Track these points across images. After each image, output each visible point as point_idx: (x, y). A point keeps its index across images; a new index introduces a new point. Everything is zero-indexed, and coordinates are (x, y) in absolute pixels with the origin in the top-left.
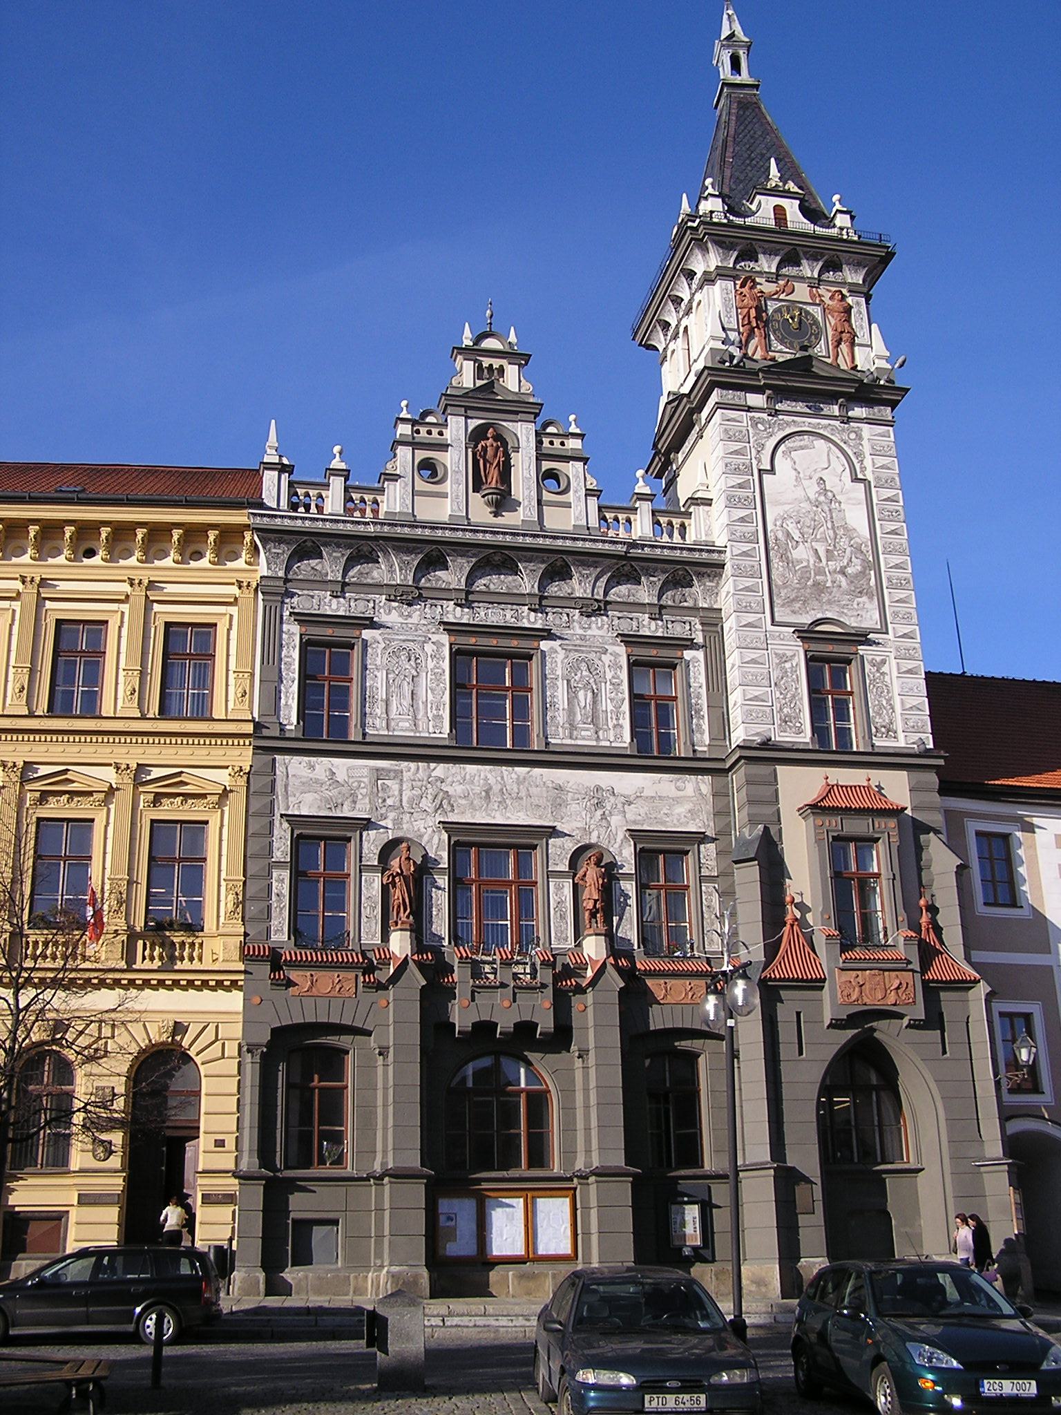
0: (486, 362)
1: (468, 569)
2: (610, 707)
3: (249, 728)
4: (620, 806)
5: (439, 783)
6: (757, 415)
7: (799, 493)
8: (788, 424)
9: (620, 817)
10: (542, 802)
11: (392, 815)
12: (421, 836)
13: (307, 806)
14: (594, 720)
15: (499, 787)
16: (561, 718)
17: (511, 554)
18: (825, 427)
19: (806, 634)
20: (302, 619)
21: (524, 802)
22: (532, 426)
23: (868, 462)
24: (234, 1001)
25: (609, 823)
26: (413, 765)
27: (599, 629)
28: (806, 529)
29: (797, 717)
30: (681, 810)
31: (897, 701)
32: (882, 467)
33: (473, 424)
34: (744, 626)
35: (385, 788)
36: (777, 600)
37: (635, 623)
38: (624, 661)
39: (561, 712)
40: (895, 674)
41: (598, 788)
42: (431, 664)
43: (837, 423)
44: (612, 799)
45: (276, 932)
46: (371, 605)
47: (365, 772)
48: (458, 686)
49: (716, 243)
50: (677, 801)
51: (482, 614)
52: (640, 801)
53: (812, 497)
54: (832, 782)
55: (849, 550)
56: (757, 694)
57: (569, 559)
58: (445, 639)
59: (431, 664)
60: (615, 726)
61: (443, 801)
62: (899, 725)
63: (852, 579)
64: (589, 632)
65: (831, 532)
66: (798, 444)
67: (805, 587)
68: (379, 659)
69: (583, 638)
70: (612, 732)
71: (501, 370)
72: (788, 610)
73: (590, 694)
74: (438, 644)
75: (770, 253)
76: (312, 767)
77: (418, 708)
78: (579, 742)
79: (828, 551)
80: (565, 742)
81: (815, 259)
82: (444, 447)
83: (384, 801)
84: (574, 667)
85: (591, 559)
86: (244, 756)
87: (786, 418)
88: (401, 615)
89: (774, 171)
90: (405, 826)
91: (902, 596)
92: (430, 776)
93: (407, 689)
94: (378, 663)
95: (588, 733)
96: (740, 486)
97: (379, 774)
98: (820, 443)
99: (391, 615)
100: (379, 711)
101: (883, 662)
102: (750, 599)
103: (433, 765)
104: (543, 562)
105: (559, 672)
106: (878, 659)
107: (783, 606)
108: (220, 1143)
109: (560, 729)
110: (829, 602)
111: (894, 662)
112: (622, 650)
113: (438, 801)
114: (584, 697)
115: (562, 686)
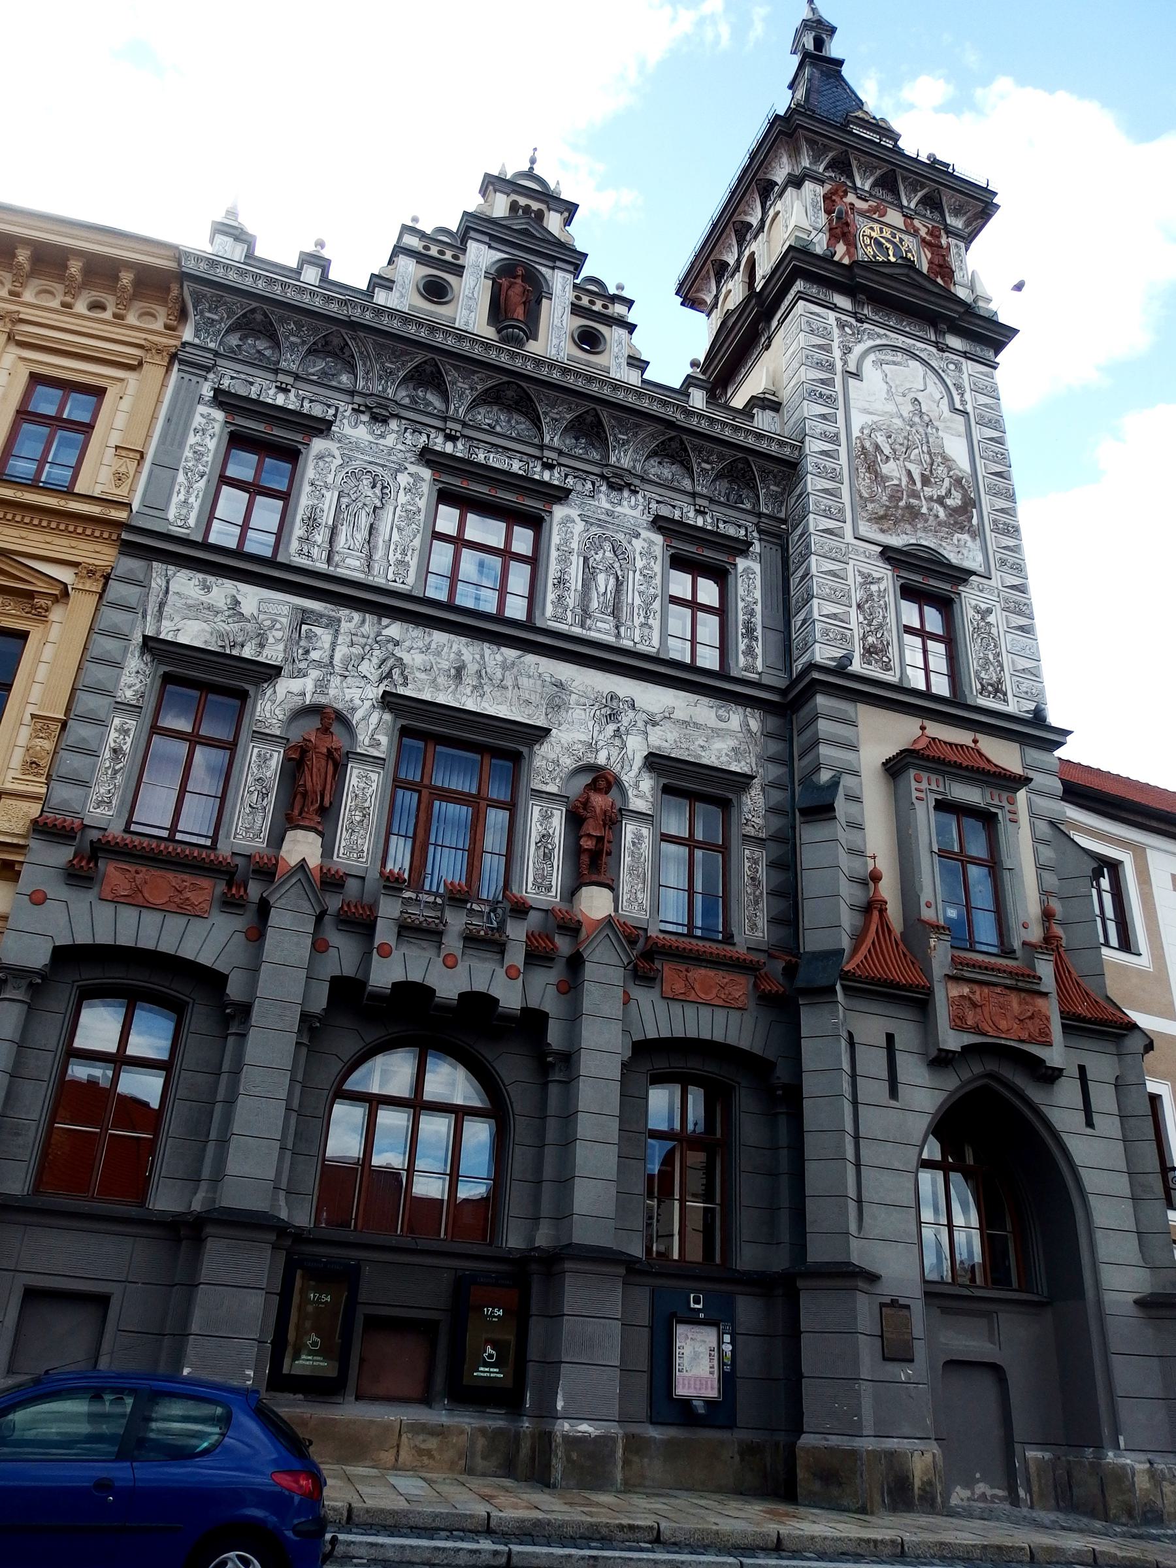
0: (523, 201)
2: (638, 601)
3: (121, 515)
4: (640, 724)
5: (390, 646)
6: (844, 318)
7: (890, 408)
8: (879, 336)
10: (533, 698)
11: (315, 674)
12: (354, 709)
14: (615, 612)
15: (476, 667)
16: (572, 600)
21: (509, 694)
22: (570, 277)
23: (967, 396)
25: (624, 746)
26: (357, 616)
27: (632, 510)
29: (884, 651)
31: (1006, 659)
41: (613, 697)
43: (934, 350)
45: (99, 804)
47: (285, 610)
49: (807, 140)
50: (717, 733)
52: (667, 725)
53: (905, 414)
55: (947, 481)
59: (403, 498)
60: (642, 625)
61: (392, 668)
62: (1008, 686)
64: (619, 509)
65: (927, 457)
66: (889, 358)
67: (897, 507)
69: (610, 513)
70: (637, 632)
72: (875, 527)
73: (612, 581)
75: (867, 170)
76: (207, 588)
77: (375, 547)
81: (914, 188)
83: (307, 652)
84: (594, 544)
87: (877, 329)
88: (372, 433)
90: (332, 692)
91: (1011, 544)
92: (379, 634)
93: (364, 521)
94: (330, 479)
95: (607, 626)
97: (304, 617)
99: (356, 431)
100: (320, 537)
101: (989, 611)
102: (831, 503)
103: (385, 621)
104: (570, 410)
105: (575, 545)
106: (984, 606)
107: (869, 520)
109: (569, 613)
110: (925, 529)
113: (385, 669)
115: (576, 563)
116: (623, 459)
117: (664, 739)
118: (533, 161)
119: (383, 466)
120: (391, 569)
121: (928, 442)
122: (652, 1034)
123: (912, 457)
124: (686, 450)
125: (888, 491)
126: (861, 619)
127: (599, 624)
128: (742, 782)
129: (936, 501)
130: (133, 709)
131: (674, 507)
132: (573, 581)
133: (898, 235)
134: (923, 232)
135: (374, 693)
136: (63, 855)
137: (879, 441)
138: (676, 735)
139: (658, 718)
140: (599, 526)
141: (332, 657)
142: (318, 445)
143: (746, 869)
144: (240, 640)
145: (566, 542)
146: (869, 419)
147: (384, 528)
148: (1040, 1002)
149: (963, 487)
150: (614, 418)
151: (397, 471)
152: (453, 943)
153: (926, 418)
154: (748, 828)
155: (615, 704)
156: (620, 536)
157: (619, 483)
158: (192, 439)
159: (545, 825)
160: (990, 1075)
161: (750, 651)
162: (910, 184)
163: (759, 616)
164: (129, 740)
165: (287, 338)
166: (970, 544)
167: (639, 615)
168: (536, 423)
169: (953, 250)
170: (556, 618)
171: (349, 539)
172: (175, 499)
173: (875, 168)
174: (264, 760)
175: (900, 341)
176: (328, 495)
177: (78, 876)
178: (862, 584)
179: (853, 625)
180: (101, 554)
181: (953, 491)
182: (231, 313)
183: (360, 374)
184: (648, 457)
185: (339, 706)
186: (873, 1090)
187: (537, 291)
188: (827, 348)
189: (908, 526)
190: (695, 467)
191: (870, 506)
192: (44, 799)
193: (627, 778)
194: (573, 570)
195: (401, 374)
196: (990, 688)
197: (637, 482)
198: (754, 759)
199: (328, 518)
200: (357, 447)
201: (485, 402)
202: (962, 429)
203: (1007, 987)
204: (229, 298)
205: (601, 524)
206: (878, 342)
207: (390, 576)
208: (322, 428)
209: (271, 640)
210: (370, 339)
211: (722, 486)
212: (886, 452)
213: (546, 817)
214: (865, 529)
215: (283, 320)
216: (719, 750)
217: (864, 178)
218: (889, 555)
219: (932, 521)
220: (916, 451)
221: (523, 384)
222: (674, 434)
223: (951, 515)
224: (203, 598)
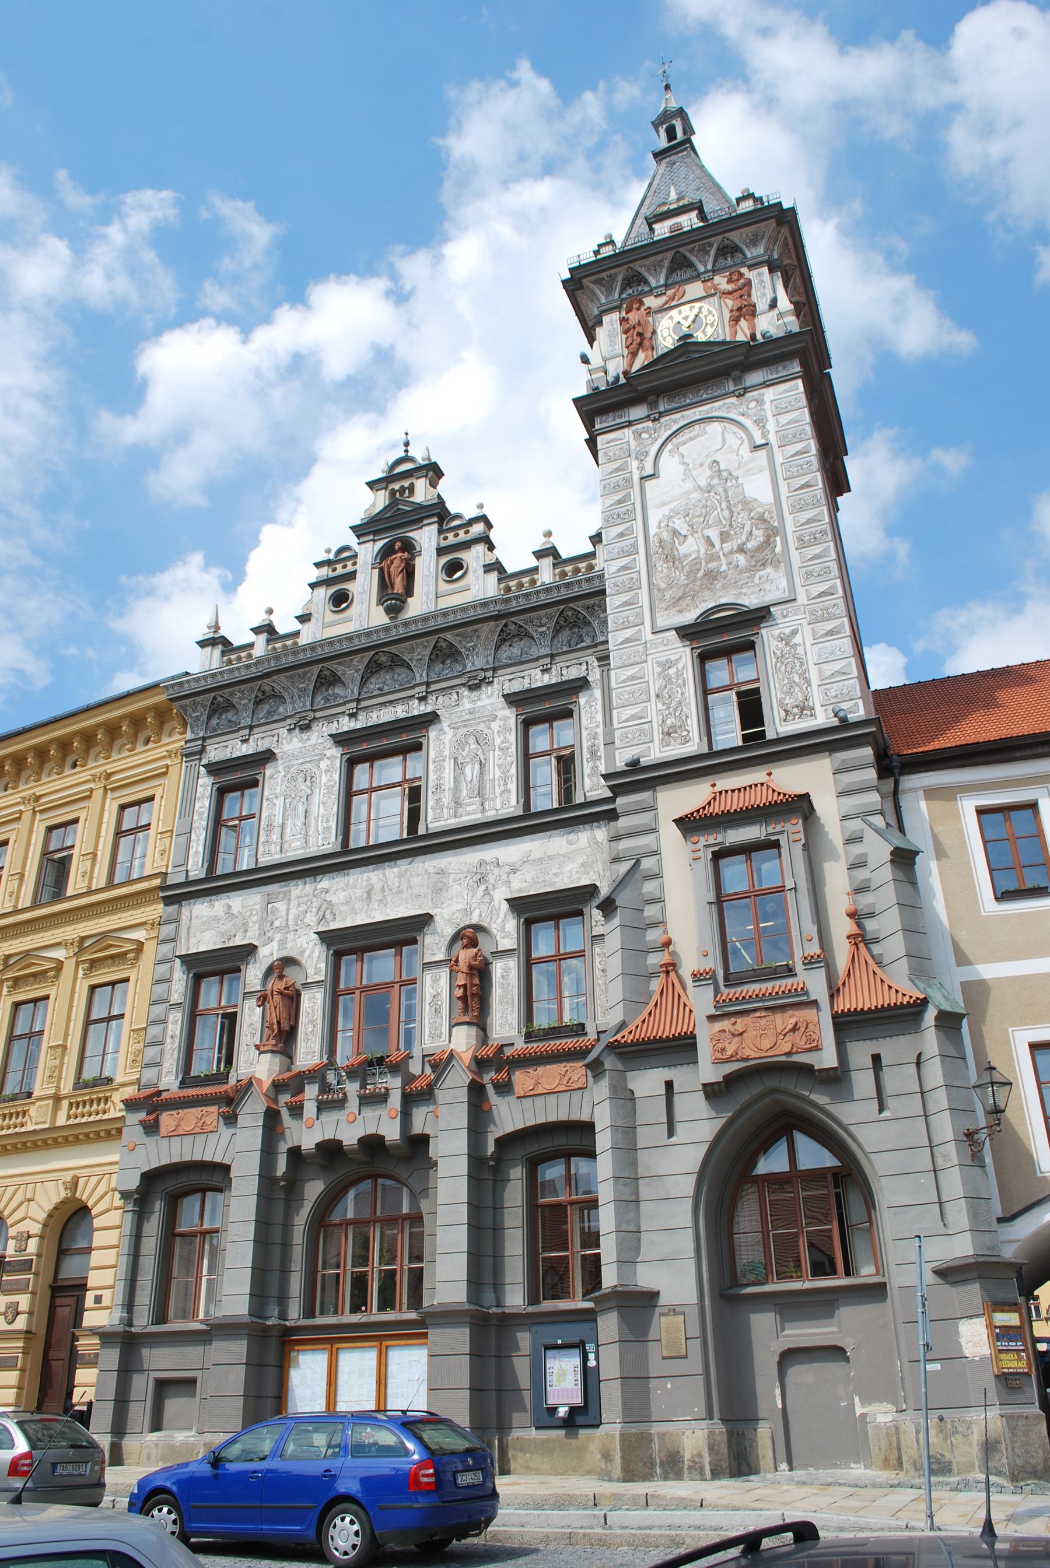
1: (359, 679)
2: (498, 774)
4: (504, 877)
5: (323, 895)
7: (690, 485)
8: (675, 422)
9: (504, 889)
11: (278, 937)
12: (303, 952)
13: (204, 941)
15: (381, 884)
16: (447, 798)
17: (392, 649)
18: (720, 408)
20: (214, 769)
21: (404, 895)
23: (771, 426)
27: (490, 698)
28: (696, 520)
32: (789, 423)
33: (380, 544)
34: (621, 643)
37: (527, 681)
39: (446, 793)
40: (809, 640)
43: (733, 400)
44: (496, 871)
46: (276, 739)
49: (594, 282)
50: (568, 856)
51: (375, 717)
53: (703, 483)
54: (717, 789)
56: (633, 712)
57: (448, 636)
59: (324, 779)
60: (502, 793)
62: (817, 700)
64: (479, 704)
65: (726, 513)
68: (278, 788)
69: (472, 712)
70: (498, 800)
72: (673, 611)
73: (477, 767)
75: (655, 269)
77: (309, 826)
78: (464, 819)
79: (722, 534)
80: (450, 822)
82: (351, 576)
83: (272, 923)
84: (461, 744)
85: (469, 629)
88: (301, 740)
90: (289, 945)
94: (278, 791)
95: (474, 807)
96: (620, 502)
98: (715, 427)
99: (290, 745)
100: (275, 837)
101: (794, 633)
105: (447, 753)
106: (787, 631)
107: (666, 609)
108: (98, 1299)
109: (445, 811)
110: (724, 587)
111: (807, 630)
113: (321, 913)
114: (471, 771)
115: (449, 765)
119: (309, 762)
120: (320, 837)
121: (727, 497)
123: (710, 522)
124: (521, 626)
125: (687, 569)
126: (660, 706)
127: (469, 808)
129: (736, 552)
131: (523, 677)
132: (446, 784)
136: (142, 1115)
137: (676, 526)
138: (533, 872)
139: (517, 866)
140: (465, 726)
141: (287, 920)
143: (597, 964)
144: (233, 933)
145: (440, 753)
146: (666, 511)
147: (314, 810)
148: (807, 1014)
149: (765, 521)
150: (457, 635)
151: (320, 760)
152: (353, 1102)
153: (725, 474)
154: (597, 929)
155: (483, 868)
156: (482, 726)
160: (773, 1091)
162: (699, 250)
163: (601, 737)
164: (179, 1027)
165: (239, 703)
167: (499, 785)
168: (409, 667)
170: (436, 819)
172: (191, 853)
173: (662, 260)
176: (277, 802)
178: (659, 674)
180: (156, 910)
181: (755, 532)
182: (204, 706)
183: (288, 701)
184: (497, 648)
186: (651, 1134)
189: (707, 593)
190: (534, 634)
191: (668, 595)
192: (138, 1081)
193: (494, 928)
194: (446, 774)
195: (311, 687)
196: (795, 710)
197: (490, 674)
198: (601, 867)
199: (279, 820)
200: (294, 757)
201: (373, 673)
202: (764, 462)
203: (767, 1009)
204: (198, 699)
205: (466, 724)
207: (320, 843)
208: (267, 757)
209: (251, 924)
210: (281, 677)
212: (683, 533)
214: (664, 620)
215: (231, 694)
216: (570, 872)
217: (656, 276)
218: (686, 633)
219: (732, 574)
220: (716, 513)
221: (385, 649)
222: (504, 622)
223: (752, 557)
224: (211, 914)
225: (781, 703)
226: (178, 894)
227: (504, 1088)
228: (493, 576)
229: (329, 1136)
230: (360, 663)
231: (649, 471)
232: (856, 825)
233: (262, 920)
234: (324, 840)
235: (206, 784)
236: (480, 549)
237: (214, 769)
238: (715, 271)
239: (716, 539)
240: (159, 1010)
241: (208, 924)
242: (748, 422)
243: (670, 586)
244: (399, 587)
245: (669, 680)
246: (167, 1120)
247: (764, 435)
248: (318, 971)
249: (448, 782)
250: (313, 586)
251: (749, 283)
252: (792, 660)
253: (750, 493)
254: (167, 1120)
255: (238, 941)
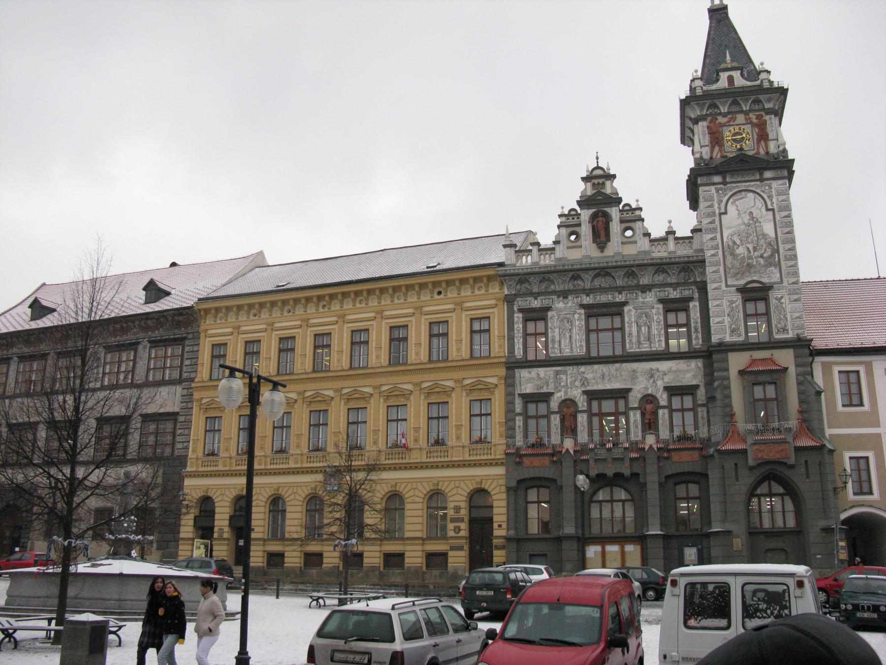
0: (596, 181)
6: (719, 186)
7: (740, 221)
8: (734, 188)
13: (529, 389)
16: (634, 340)
18: (753, 186)
19: (742, 290)
23: (774, 200)
24: (501, 471)
26: (571, 368)
27: (650, 298)
29: (738, 329)
30: (689, 375)
31: (789, 316)
33: (592, 211)
35: (560, 378)
36: (729, 275)
38: (661, 311)
41: (651, 369)
42: (577, 323)
43: (758, 183)
48: (588, 331)
50: (688, 371)
53: (746, 222)
58: (583, 311)
59: (577, 323)
62: (789, 327)
63: (766, 259)
69: (643, 303)
71: (603, 183)
74: (580, 314)
75: (724, 104)
76: (530, 373)
82: (579, 225)
84: (640, 317)
86: (502, 372)
89: (728, 57)
93: (568, 335)
96: (710, 223)
98: (751, 195)
99: (560, 304)
101: (782, 297)
108: (500, 526)
110: (755, 272)
111: (787, 297)
112: (661, 306)
114: (644, 329)
115: (634, 326)
116: (645, 280)
117: (670, 380)
118: (597, 158)
122: (670, 473)
128: (696, 387)
130: (519, 414)
133: (742, 127)
134: (754, 121)
135: (580, 391)
142: (550, 314)
145: (630, 319)
146: (730, 231)
147: (574, 336)
156: (647, 310)
157: (645, 289)
158: (516, 326)
159: (636, 417)
161: (697, 336)
166: (775, 271)
168: (613, 278)
169: (768, 122)
171: (565, 343)
174: (555, 419)
175: (743, 186)
177: (519, 464)
179: (726, 323)
185: (571, 397)
187: (607, 218)
188: (711, 206)
189: (748, 274)
199: (557, 338)
200: (560, 310)
202: (771, 217)
206: (734, 191)
208: (549, 309)
210: (555, 275)
211: (682, 275)
213: (635, 415)
217: (724, 106)
225: (776, 326)
226: (513, 365)
227: (667, 458)
228: (647, 239)
229: (601, 471)
230: (592, 273)
231: (723, 210)
232: (801, 378)
233: (555, 382)
234: (579, 350)
235: (518, 317)
236: (640, 223)
237: (520, 310)
238: (751, 111)
239: (751, 249)
240: (510, 415)
241: (530, 380)
242: (765, 196)
243: (733, 267)
244: (603, 238)
245: (733, 309)
246: (526, 461)
247: (772, 204)
248: (583, 406)
249: (635, 333)
250: (559, 227)
251: (765, 122)
252: (781, 309)
253: (766, 231)
254: (526, 461)
255: (545, 390)
